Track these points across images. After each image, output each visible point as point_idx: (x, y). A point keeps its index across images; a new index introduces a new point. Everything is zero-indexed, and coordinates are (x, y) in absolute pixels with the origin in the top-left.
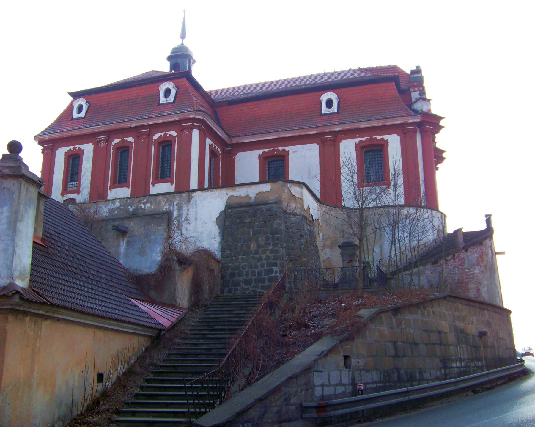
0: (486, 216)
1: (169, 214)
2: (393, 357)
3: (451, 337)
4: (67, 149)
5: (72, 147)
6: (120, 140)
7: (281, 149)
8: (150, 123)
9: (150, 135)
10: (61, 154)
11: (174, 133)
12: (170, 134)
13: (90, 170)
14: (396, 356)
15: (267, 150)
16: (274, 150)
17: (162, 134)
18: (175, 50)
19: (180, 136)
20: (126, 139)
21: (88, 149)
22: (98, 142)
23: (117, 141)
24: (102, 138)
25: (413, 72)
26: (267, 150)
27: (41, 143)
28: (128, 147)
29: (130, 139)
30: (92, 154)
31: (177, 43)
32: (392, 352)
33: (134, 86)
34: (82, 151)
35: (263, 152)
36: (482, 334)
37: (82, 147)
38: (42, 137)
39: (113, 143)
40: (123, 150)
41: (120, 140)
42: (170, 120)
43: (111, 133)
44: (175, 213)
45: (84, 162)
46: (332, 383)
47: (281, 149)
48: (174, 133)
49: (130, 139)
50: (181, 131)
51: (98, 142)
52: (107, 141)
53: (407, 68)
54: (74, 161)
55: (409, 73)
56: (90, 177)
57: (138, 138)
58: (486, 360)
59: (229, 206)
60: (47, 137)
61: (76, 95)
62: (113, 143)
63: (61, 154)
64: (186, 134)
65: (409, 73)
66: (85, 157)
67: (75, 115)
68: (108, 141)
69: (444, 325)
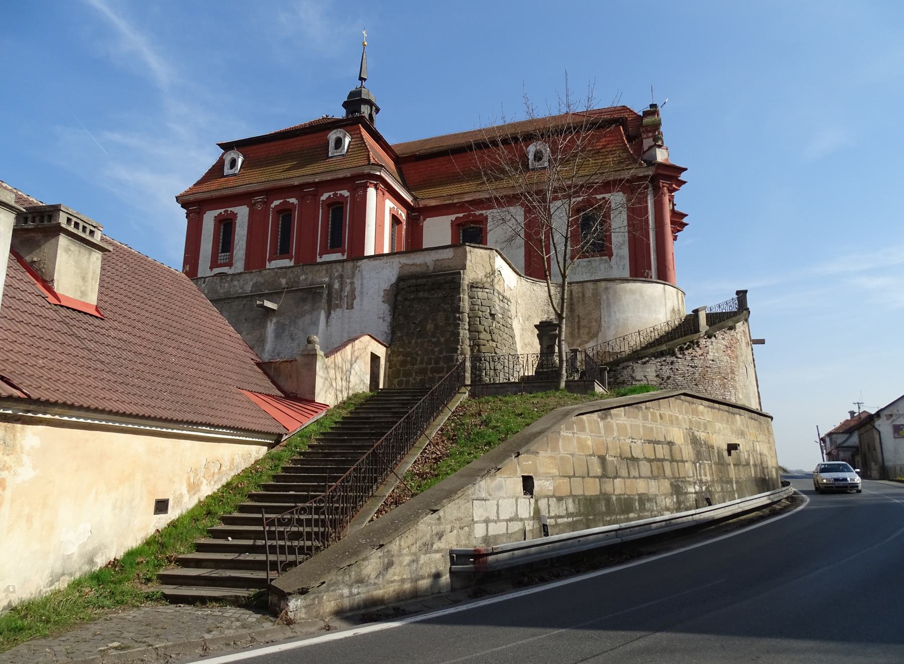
0: (738, 293)
1: (330, 286)
2: (600, 478)
3: (688, 452)
4: (217, 212)
5: (222, 211)
7: (477, 213)
8: (317, 180)
9: (316, 195)
10: (209, 219)
11: (346, 193)
13: (245, 238)
14: (604, 476)
15: (461, 215)
16: (469, 215)
17: (331, 193)
18: (352, 94)
19: (353, 196)
21: (242, 213)
22: (254, 204)
25: (646, 114)
26: (461, 215)
28: (290, 210)
29: (293, 200)
30: (247, 218)
31: (355, 85)
32: (598, 471)
33: (298, 136)
34: (235, 215)
35: (457, 218)
36: (732, 447)
37: (235, 210)
39: (273, 206)
40: (285, 213)
42: (341, 176)
43: (271, 193)
44: (336, 286)
45: (237, 229)
46: (501, 518)
47: (477, 213)
48: (346, 193)
49: (293, 200)
50: (353, 190)
52: (265, 203)
53: (639, 108)
54: (226, 226)
55: (641, 114)
56: (244, 247)
57: (301, 199)
58: (737, 482)
59: (401, 279)
60: (192, 198)
61: (227, 147)
62: (273, 206)
63: (209, 219)
64: (360, 193)
65: (641, 114)
66: (238, 221)
67: (227, 171)
69: (677, 435)
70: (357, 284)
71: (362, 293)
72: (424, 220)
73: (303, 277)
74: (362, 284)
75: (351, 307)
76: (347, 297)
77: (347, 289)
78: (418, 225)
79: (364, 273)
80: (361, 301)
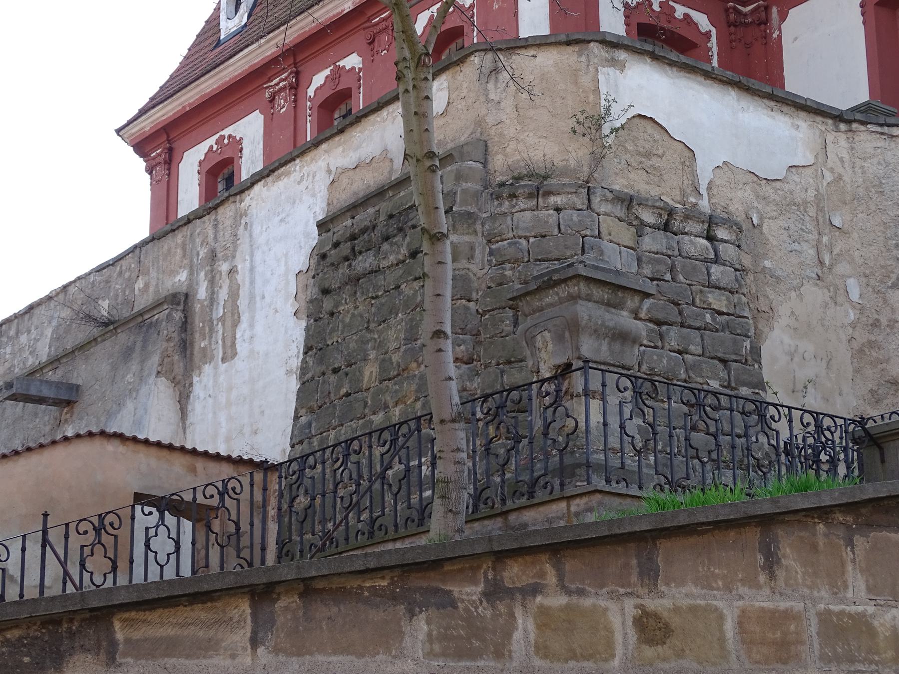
1: (181, 300)
5: (212, 141)
6: (327, 72)
12: (686, 16)
20: (341, 63)
22: (272, 100)
23: (319, 80)
24: (280, 81)
27: (141, 147)
29: (353, 61)
38: (135, 129)
39: (311, 92)
41: (327, 72)
44: (202, 293)
49: (353, 61)
51: (272, 100)
60: (147, 125)
62: (311, 92)
68: (296, 88)
70: (242, 277)
71: (252, 297)
72: (783, 17)
73: (140, 284)
74: (252, 269)
75: (230, 354)
76: (222, 319)
77: (223, 294)
78: (766, 37)
79: (256, 229)
80: (252, 326)
